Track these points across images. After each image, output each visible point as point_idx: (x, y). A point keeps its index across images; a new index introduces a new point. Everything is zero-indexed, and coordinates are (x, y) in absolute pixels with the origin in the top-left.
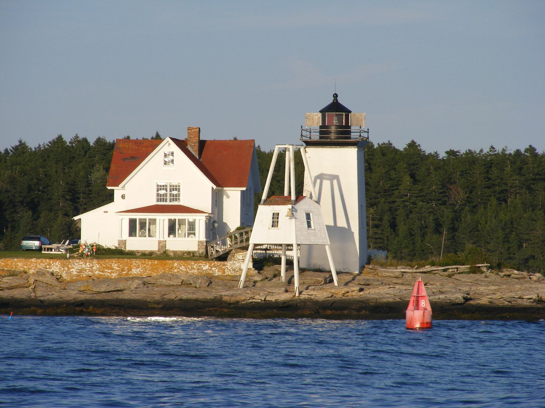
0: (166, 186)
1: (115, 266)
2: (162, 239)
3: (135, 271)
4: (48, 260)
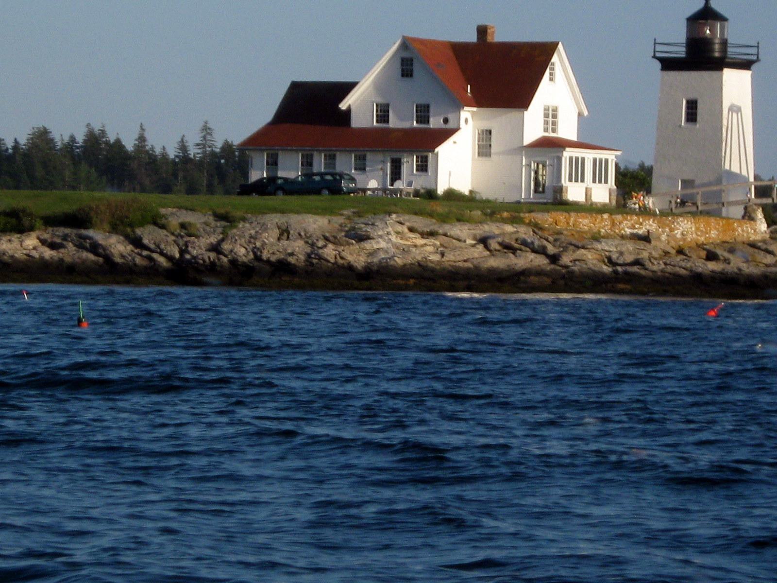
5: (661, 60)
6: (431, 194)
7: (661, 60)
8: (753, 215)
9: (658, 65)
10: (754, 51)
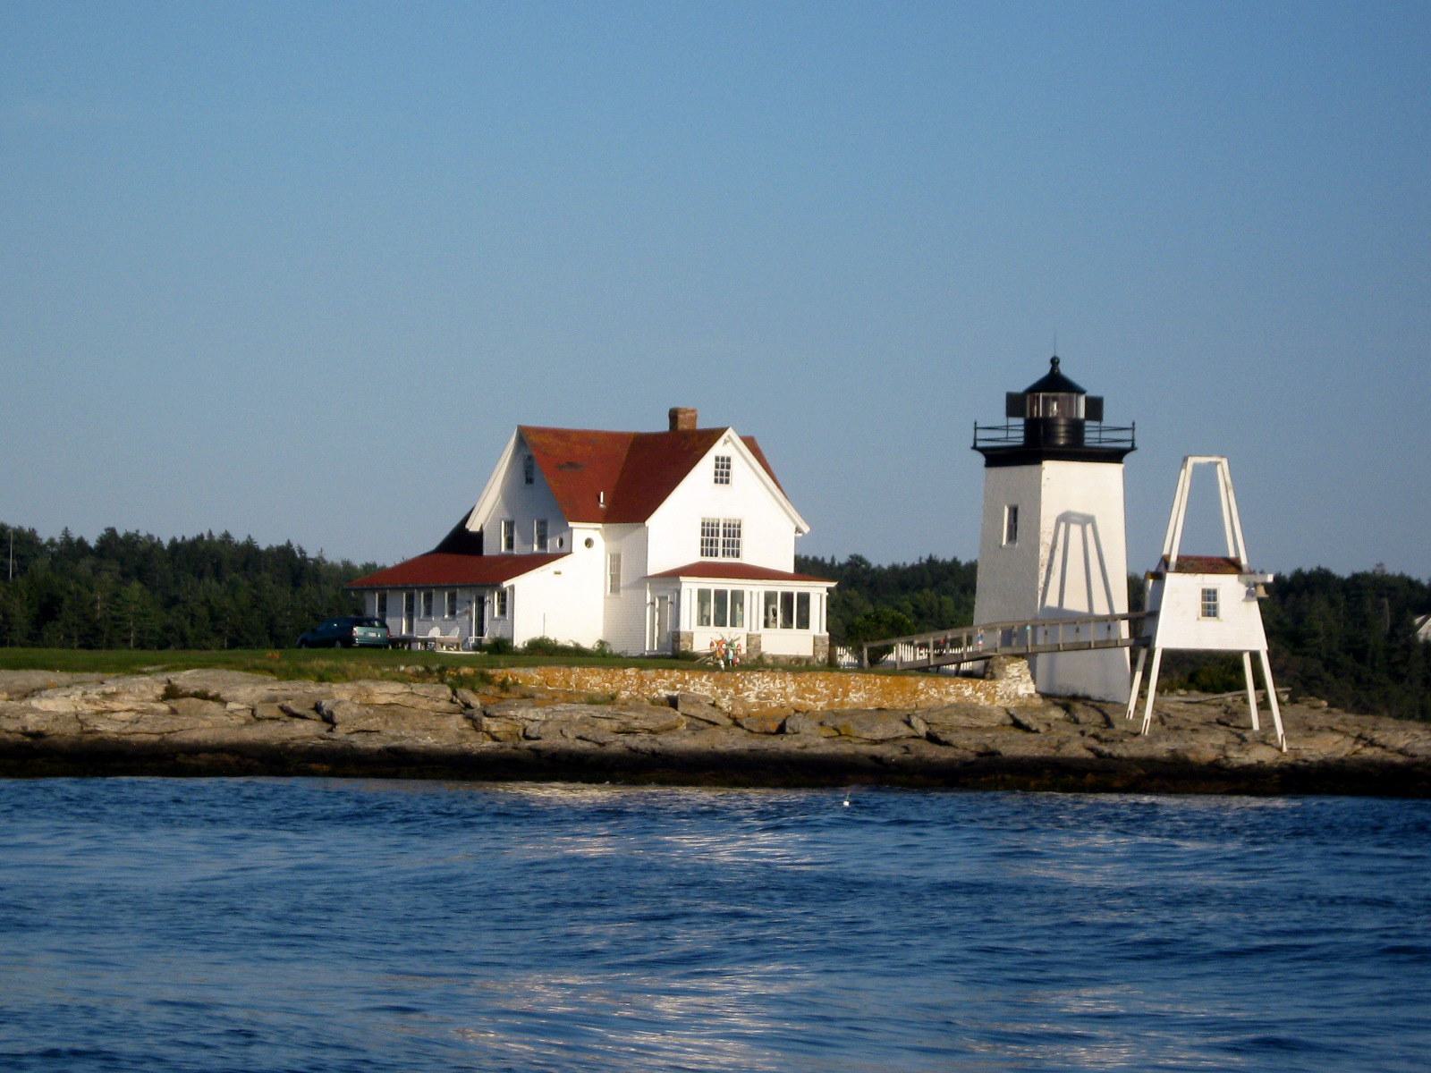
0: (718, 525)
1: (820, 686)
2: (754, 632)
3: (856, 698)
4: (676, 674)
5: (982, 450)
6: (501, 647)
7: (982, 450)
8: (996, 671)
9: (981, 459)
10: (1127, 435)
